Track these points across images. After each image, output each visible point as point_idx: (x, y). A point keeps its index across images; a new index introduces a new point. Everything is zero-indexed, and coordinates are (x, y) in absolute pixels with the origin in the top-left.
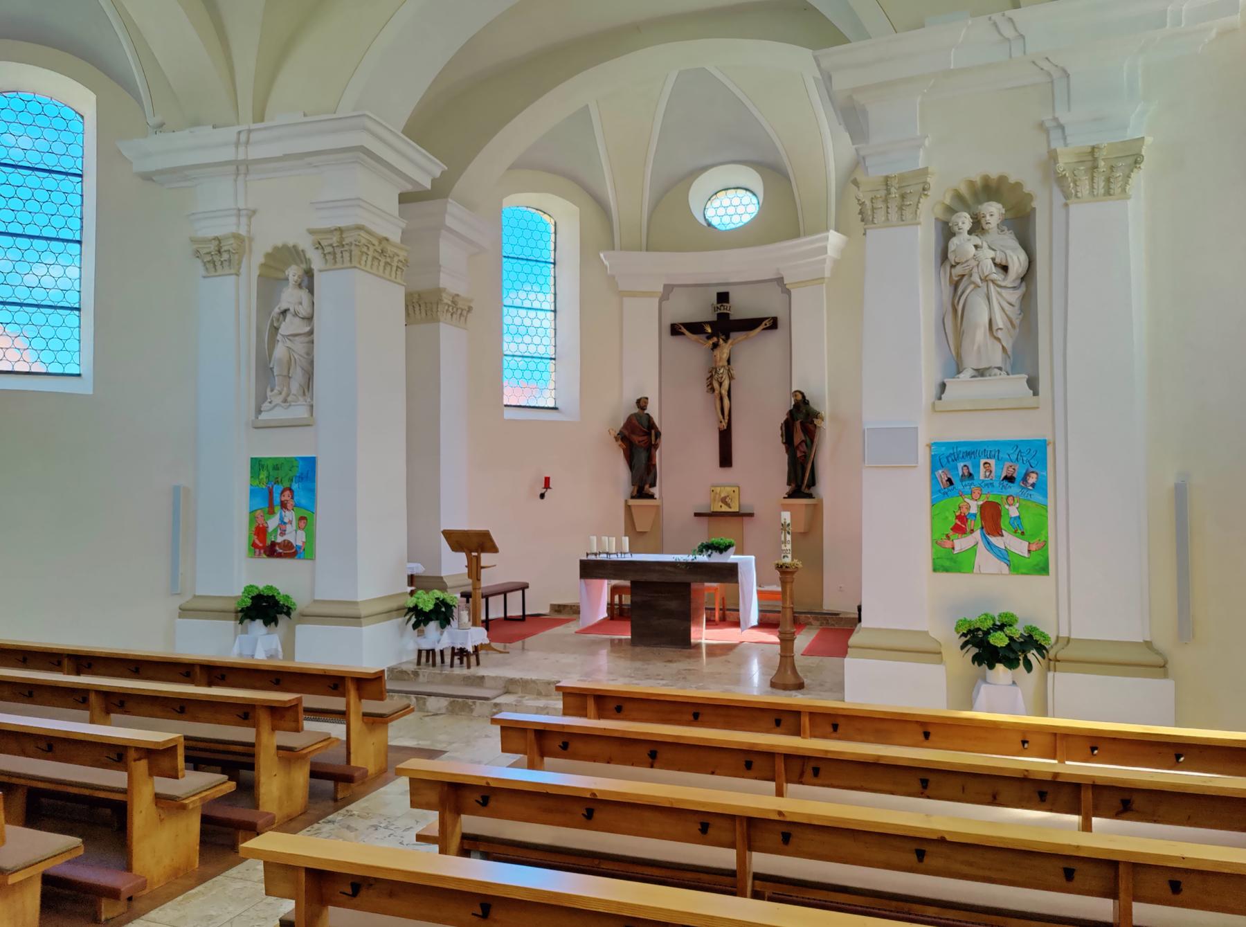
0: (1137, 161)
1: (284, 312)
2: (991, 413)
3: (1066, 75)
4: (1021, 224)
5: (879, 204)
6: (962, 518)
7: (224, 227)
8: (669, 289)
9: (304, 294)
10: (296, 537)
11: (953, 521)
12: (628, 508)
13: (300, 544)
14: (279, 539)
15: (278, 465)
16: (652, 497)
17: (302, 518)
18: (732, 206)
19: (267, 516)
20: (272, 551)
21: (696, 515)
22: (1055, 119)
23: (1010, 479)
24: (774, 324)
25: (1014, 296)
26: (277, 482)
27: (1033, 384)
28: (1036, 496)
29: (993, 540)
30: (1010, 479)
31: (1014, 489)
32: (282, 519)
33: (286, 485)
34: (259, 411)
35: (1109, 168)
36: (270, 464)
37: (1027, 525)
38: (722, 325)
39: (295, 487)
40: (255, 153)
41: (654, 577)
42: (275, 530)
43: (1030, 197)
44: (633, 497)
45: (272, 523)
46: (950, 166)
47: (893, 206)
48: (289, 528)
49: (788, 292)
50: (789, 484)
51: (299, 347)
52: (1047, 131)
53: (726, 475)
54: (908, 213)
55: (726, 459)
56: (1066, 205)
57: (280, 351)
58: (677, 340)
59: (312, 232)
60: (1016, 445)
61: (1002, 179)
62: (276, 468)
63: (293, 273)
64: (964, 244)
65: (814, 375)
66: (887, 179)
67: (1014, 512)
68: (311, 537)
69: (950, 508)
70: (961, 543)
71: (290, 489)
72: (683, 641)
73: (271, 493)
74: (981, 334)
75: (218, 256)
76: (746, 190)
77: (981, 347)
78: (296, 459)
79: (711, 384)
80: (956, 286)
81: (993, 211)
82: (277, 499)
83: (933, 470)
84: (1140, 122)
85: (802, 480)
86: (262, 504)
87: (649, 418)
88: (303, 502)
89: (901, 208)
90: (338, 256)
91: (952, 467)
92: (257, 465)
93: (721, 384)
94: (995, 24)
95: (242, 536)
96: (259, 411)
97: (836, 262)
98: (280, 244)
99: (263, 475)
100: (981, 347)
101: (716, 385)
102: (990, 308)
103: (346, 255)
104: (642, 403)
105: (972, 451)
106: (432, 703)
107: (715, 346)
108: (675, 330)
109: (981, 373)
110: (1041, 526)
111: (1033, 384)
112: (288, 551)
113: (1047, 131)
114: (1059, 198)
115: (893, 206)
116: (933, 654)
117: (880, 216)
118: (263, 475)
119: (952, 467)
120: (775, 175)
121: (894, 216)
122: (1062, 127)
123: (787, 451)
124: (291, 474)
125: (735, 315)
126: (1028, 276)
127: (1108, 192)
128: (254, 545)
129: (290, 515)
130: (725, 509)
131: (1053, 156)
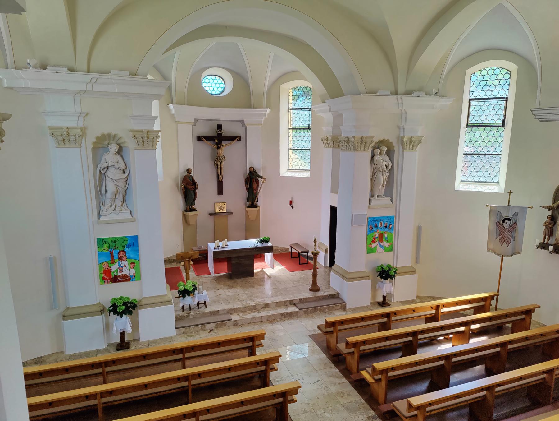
0: (420, 142)
1: (108, 168)
2: (382, 208)
3: (406, 113)
4: (390, 153)
5: (359, 145)
6: (374, 238)
7: (72, 122)
8: (196, 120)
9: (119, 157)
10: (130, 272)
11: (372, 239)
12: (184, 216)
13: (132, 275)
14: (119, 274)
15: (114, 241)
16: (194, 210)
17: (132, 263)
18: (214, 84)
19: (110, 265)
20: (115, 280)
21: (210, 215)
22: (403, 126)
23: (386, 227)
24: (240, 140)
25: (388, 175)
26: (115, 248)
27: (392, 200)
28: (391, 231)
29: (382, 244)
30: (386, 227)
31: (387, 229)
32: (120, 266)
33: (121, 249)
34: (99, 215)
35: (413, 143)
36: (110, 241)
37: (389, 239)
38: (217, 138)
39: (126, 250)
40: (97, 88)
41: (243, 254)
42: (116, 270)
43: (394, 147)
44: (186, 211)
45: (114, 267)
46: (377, 135)
47: (363, 145)
48: (124, 268)
49: (246, 127)
50: (248, 201)
51: (121, 184)
52: (399, 129)
53: (220, 198)
54: (366, 149)
55: (220, 192)
56: (403, 151)
57: (111, 187)
58: (200, 143)
59: (132, 131)
60: (388, 217)
61: (388, 140)
62: (114, 242)
63: (114, 148)
64: (377, 158)
65: (256, 160)
66: (362, 137)
67: (386, 236)
68: (138, 272)
69: (372, 235)
70: (374, 245)
71: (124, 251)
72: (251, 273)
73: (112, 254)
74: (381, 186)
75: (65, 137)
76: (220, 77)
77: (380, 190)
78: (126, 237)
79: (217, 163)
80: (374, 169)
81: (385, 149)
82: (116, 256)
83: (368, 226)
84: (420, 132)
85: (252, 200)
86: (106, 259)
87: (192, 178)
88: (132, 256)
89: (364, 147)
90: (146, 143)
91: (373, 224)
92: (101, 242)
93: (221, 163)
94: (397, 99)
95: (95, 274)
96: (99, 215)
97: (266, 118)
98: (106, 133)
99: (106, 246)
100: (380, 190)
101: (219, 163)
102: (382, 178)
103: (151, 144)
104: (189, 171)
105: (378, 219)
106: (208, 327)
107: (218, 148)
108: (199, 139)
109: (378, 196)
110: (392, 239)
111: (392, 200)
112: (126, 278)
113: (399, 129)
114: (401, 149)
115: (363, 145)
116: (367, 277)
117: (359, 148)
118: (106, 246)
119: (373, 224)
120: (241, 80)
121: (362, 149)
122: (404, 128)
123: (247, 189)
124: (123, 244)
125: (224, 134)
126: (391, 171)
127: (412, 149)
128: (103, 278)
129: (123, 263)
130: (221, 211)
131: (402, 138)
